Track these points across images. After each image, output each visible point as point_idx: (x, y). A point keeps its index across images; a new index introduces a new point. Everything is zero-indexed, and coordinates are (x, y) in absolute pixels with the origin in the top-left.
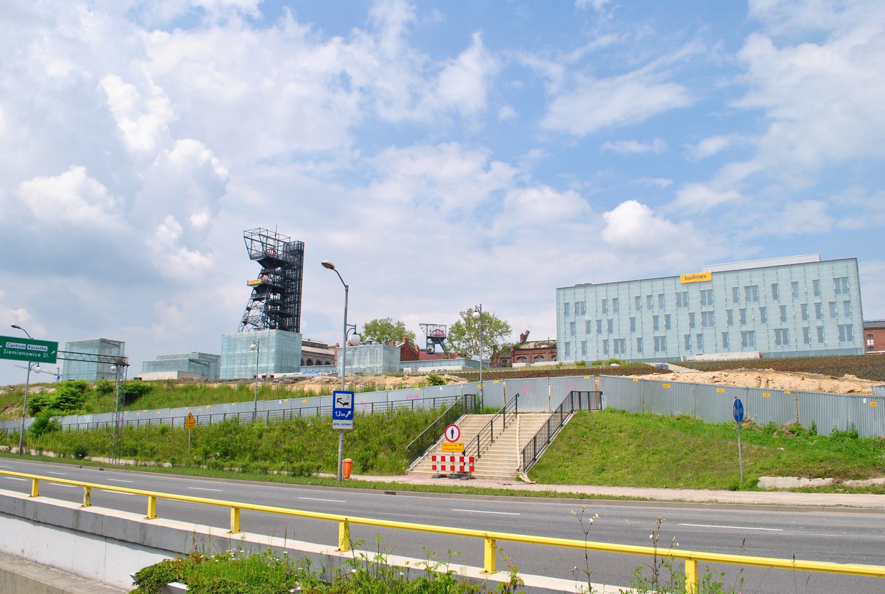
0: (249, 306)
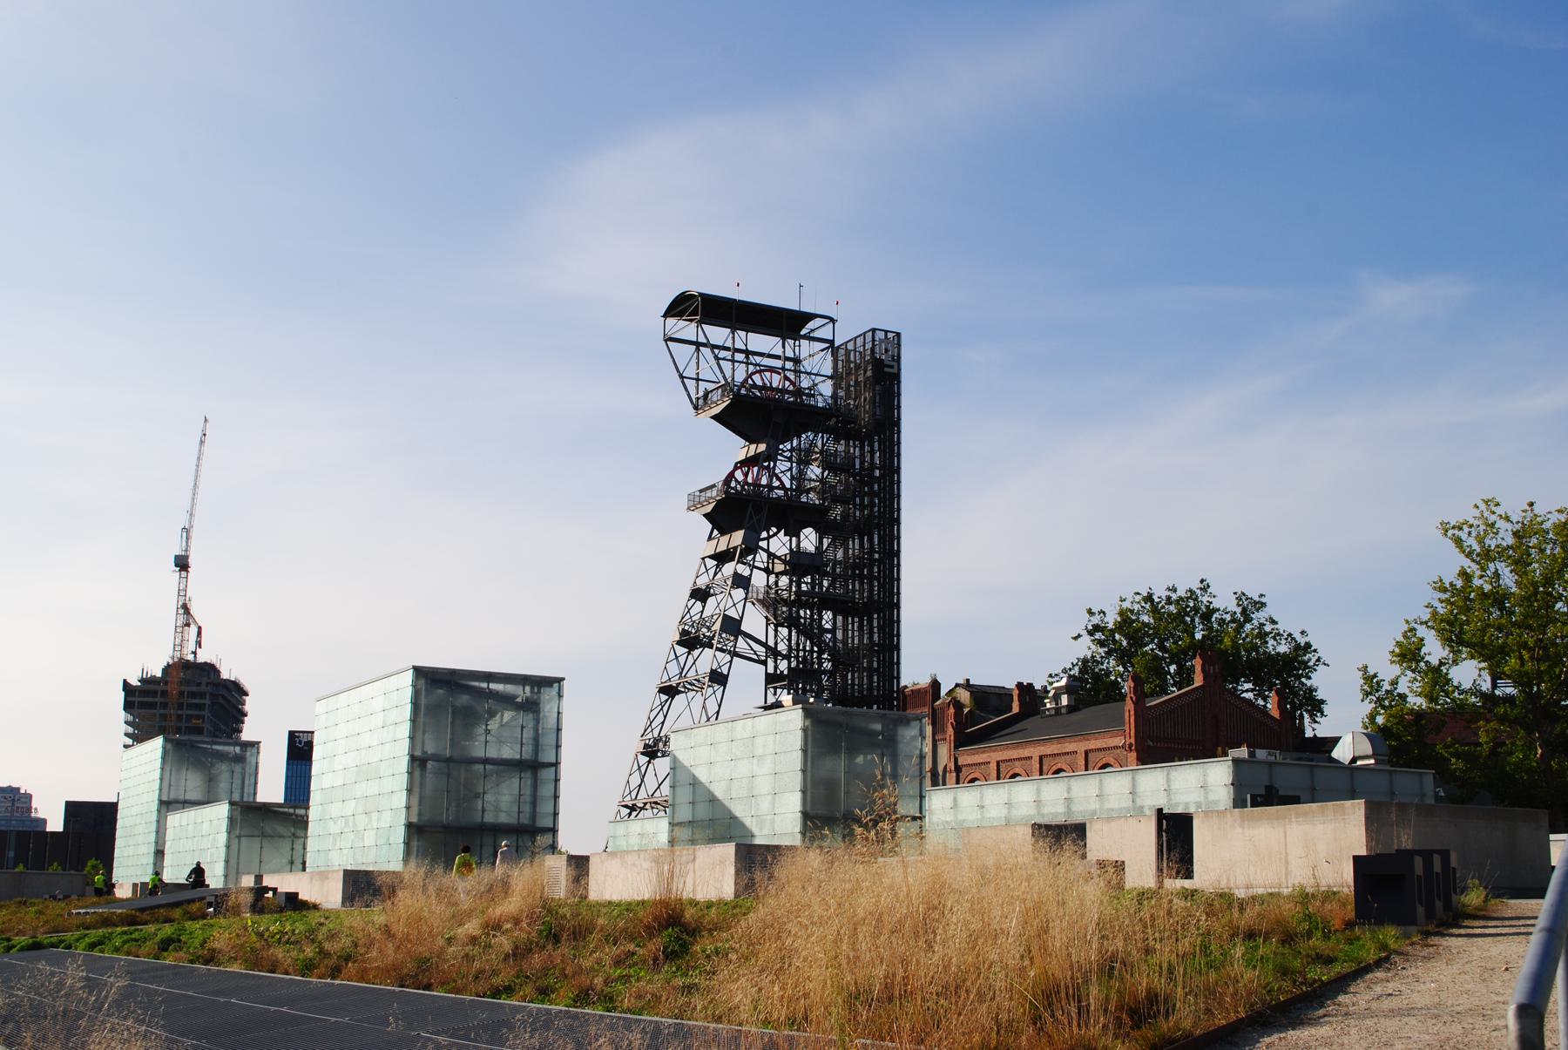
0: (702, 582)
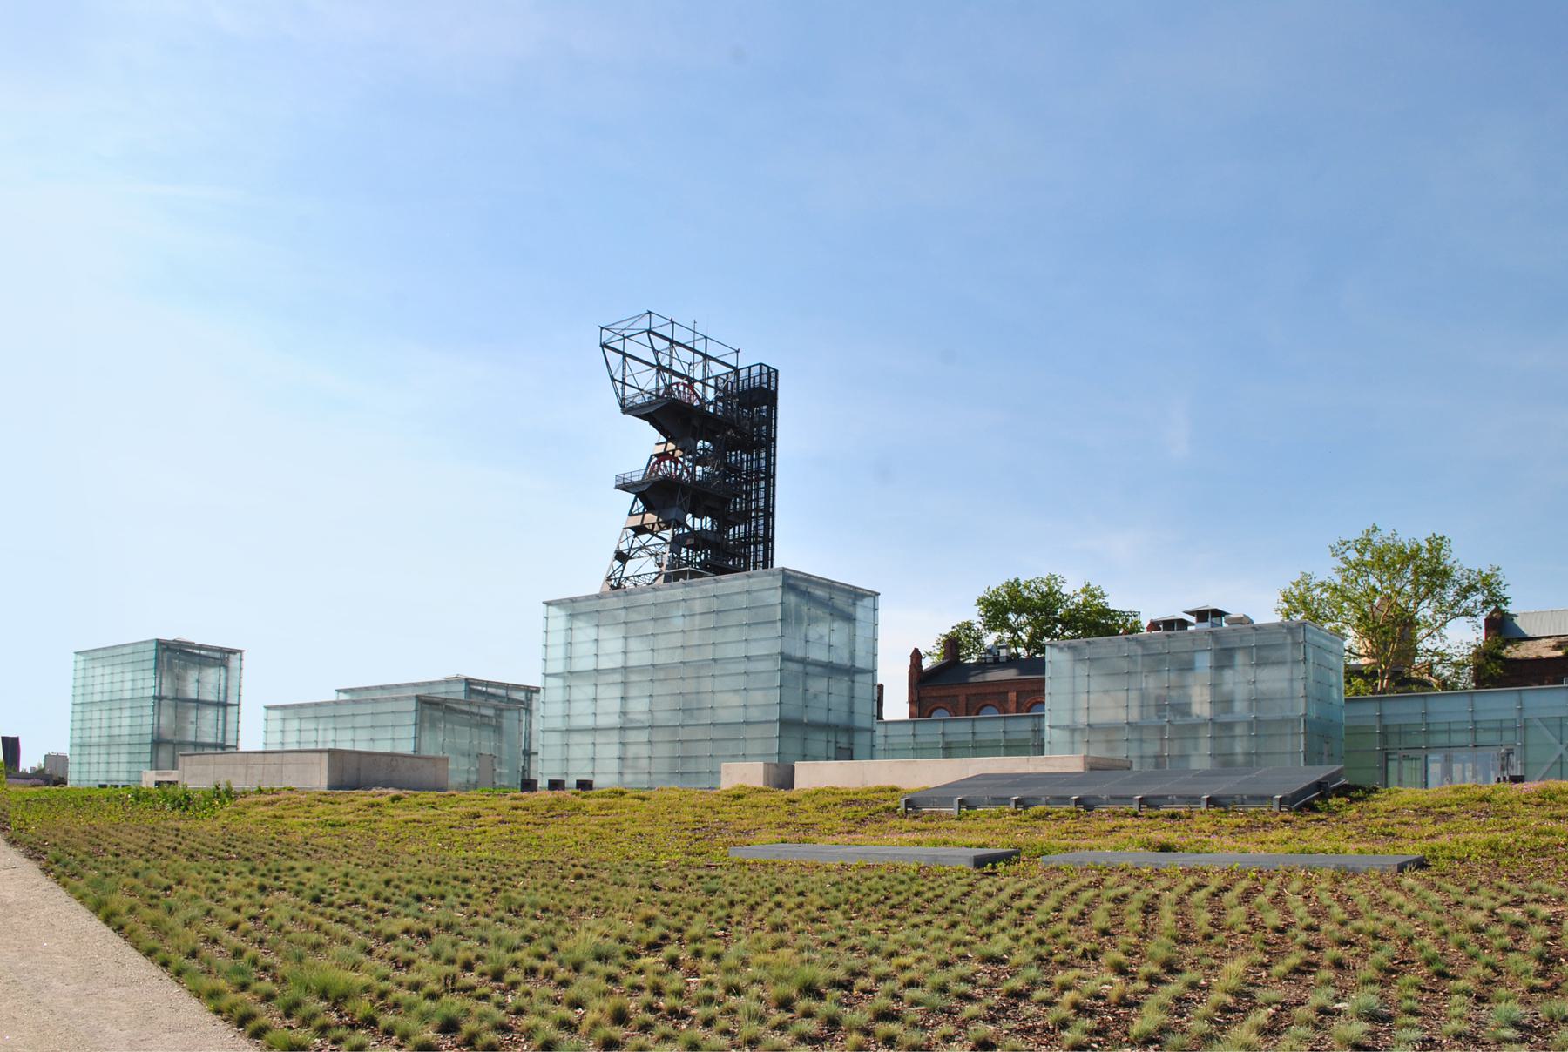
0: (624, 546)
